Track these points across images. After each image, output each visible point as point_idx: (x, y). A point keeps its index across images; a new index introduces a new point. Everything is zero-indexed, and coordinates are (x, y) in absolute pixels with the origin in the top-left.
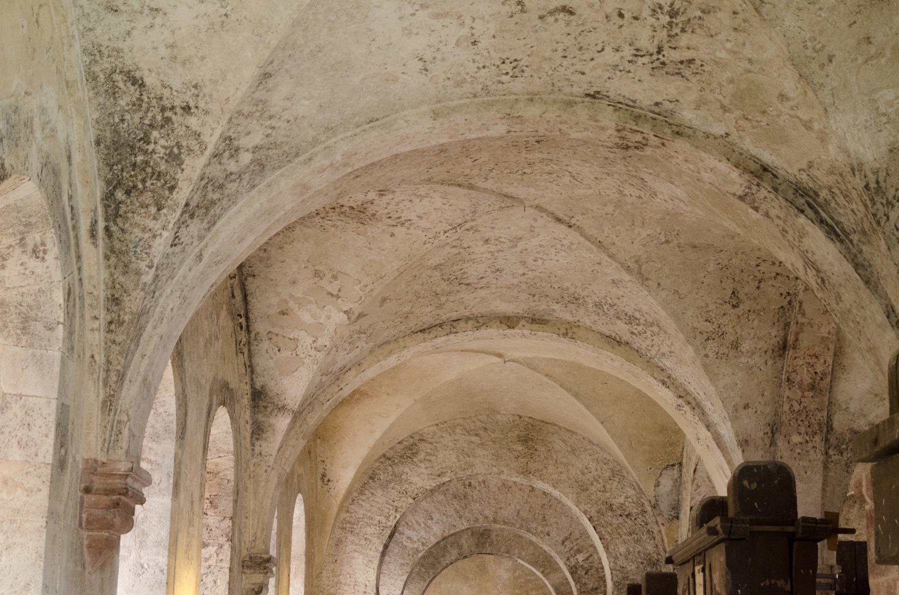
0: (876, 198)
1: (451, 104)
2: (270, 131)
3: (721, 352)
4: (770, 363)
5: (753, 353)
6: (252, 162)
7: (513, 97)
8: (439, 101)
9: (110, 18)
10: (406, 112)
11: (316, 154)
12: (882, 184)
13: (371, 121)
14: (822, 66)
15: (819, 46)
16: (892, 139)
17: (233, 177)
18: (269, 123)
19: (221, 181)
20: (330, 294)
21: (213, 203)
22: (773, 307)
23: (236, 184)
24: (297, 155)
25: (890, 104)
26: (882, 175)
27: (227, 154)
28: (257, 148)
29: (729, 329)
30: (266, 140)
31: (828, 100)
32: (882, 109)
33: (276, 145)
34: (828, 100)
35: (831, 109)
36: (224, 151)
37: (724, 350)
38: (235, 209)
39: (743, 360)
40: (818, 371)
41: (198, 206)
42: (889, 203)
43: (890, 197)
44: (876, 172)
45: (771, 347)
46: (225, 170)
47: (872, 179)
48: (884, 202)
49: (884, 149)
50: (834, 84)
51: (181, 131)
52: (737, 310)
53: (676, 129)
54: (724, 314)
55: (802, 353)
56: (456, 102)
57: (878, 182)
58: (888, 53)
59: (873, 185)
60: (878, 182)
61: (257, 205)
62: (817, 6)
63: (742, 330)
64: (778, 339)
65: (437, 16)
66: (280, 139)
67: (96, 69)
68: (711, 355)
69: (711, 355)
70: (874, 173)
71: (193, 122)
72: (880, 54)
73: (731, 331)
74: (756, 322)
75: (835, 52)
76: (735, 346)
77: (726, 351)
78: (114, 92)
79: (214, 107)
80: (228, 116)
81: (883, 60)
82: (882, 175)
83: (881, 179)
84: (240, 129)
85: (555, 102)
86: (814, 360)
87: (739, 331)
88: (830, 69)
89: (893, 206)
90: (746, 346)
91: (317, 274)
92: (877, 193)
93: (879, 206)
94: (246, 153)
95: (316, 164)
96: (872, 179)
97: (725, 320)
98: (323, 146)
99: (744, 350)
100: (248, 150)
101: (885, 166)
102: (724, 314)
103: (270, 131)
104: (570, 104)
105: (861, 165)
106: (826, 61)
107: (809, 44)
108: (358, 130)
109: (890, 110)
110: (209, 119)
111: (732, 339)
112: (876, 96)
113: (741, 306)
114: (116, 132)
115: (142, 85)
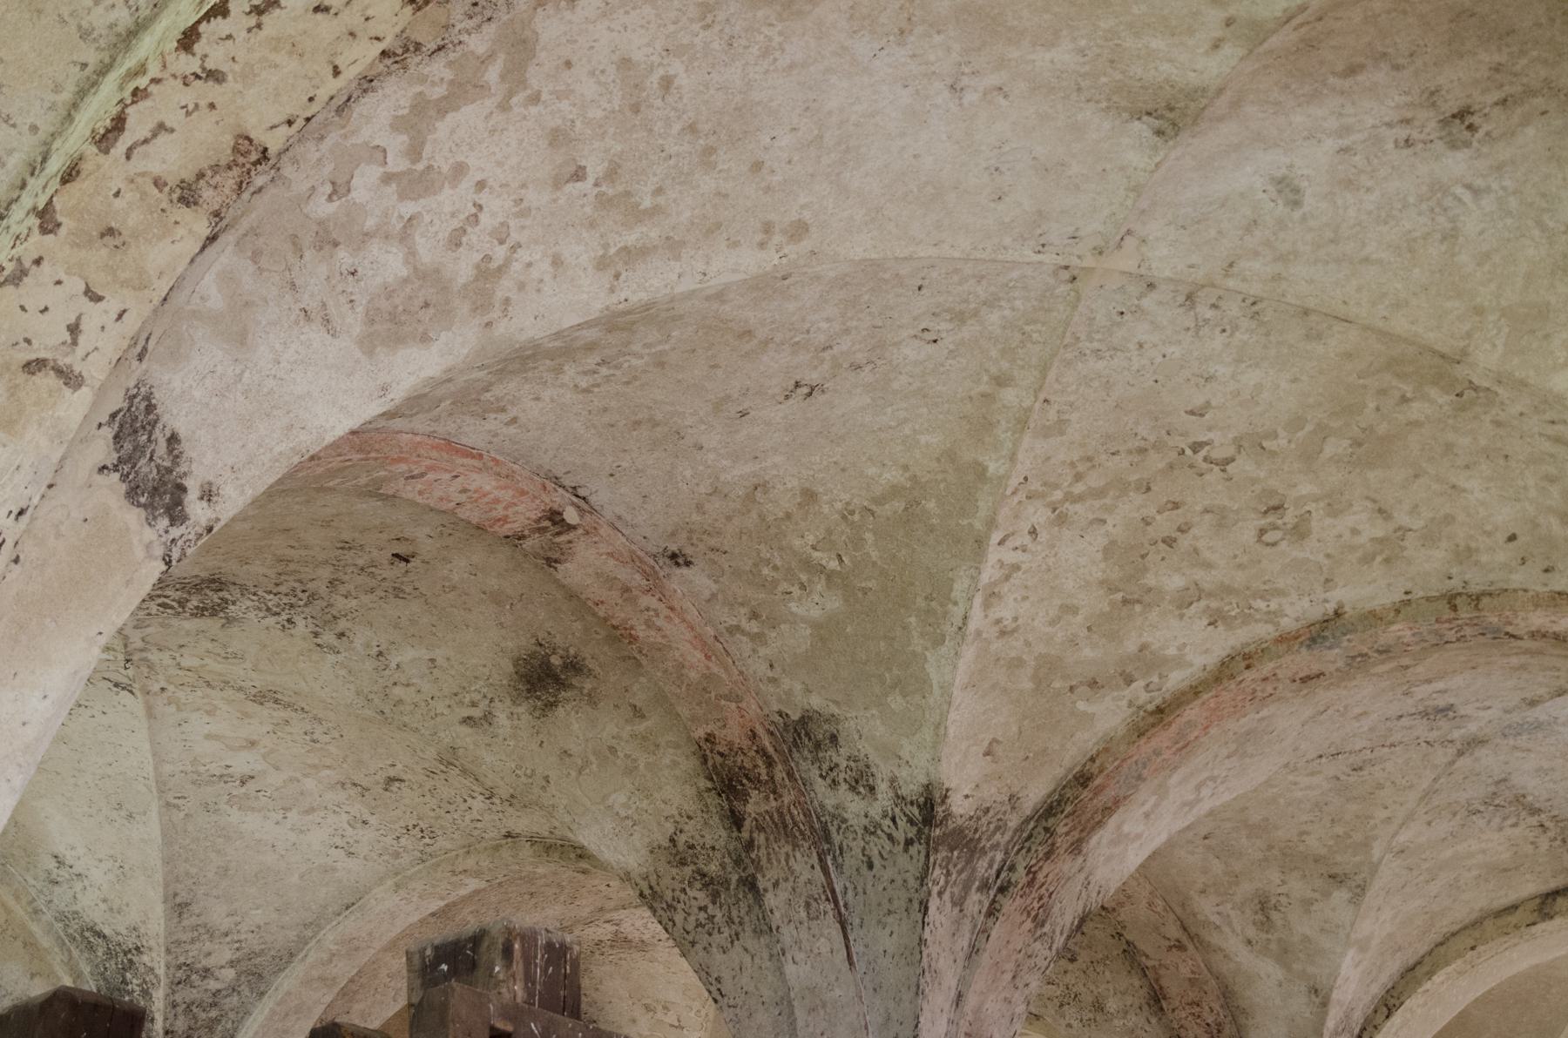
0: (655, 905)
1: (409, 873)
2: (237, 945)
3: (1085, 1018)
4: (1154, 1020)
5: (1126, 1013)
6: (239, 975)
7: (454, 853)
8: (396, 874)
9: (57, 889)
10: (374, 891)
11: (310, 950)
12: (657, 888)
13: (347, 908)
14: (543, 788)
15: (529, 772)
16: (647, 840)
17: (224, 993)
18: (228, 939)
19: (210, 1000)
20: (672, 1026)
21: (217, 1020)
22: (1115, 953)
23: (235, 998)
24: (292, 955)
25: (626, 806)
26: (653, 879)
27: (194, 977)
28: (232, 964)
29: (1080, 988)
30: (238, 954)
31: (567, 819)
32: (623, 814)
33: (252, 955)
34: (567, 819)
35: (574, 827)
36: (189, 976)
37: (1088, 1015)
38: (251, 1019)
39: (1116, 1022)
40: (1209, 1021)
41: (190, 1028)
42: (670, 906)
43: (669, 900)
44: (646, 878)
45: (1143, 1001)
46: (206, 990)
47: (644, 885)
48: (664, 906)
49: (644, 852)
50: (565, 802)
51: (142, 969)
52: (1076, 965)
53: (579, 852)
54: (1065, 972)
55: (1178, 1003)
56: (413, 870)
57: (651, 888)
58: (592, 758)
59: (647, 892)
60: (651, 888)
61: (267, 1011)
62: (501, 738)
63: (1097, 987)
64: (1145, 989)
65: (311, 810)
66: (257, 949)
67: (70, 931)
68: (1075, 1024)
69: (1075, 1024)
70: (644, 879)
71: (145, 958)
72: (587, 763)
73: (1083, 990)
74: (1107, 973)
75: (546, 773)
76: (1099, 1007)
77: (1091, 1016)
78: (91, 948)
79: (152, 943)
80: (163, 949)
81: (594, 766)
82: (653, 879)
83: (653, 883)
84: (191, 954)
85: (486, 849)
86: (1196, 1010)
87: (1093, 987)
88: (552, 789)
89: (675, 909)
90: (1112, 1005)
91: (647, 1008)
92: (653, 898)
93: (660, 912)
94: (223, 970)
95: (310, 960)
96: (644, 885)
97: (1070, 979)
98: (314, 941)
99: (1112, 1010)
100: (222, 967)
101: (652, 869)
102: (1065, 972)
103: (237, 945)
104: (497, 848)
105: (628, 873)
106: (544, 783)
107: (518, 772)
108: (341, 918)
109: (630, 812)
110: (154, 955)
111: (1091, 999)
112: (610, 802)
113: (1080, 960)
114: (105, 979)
115: (105, 937)
